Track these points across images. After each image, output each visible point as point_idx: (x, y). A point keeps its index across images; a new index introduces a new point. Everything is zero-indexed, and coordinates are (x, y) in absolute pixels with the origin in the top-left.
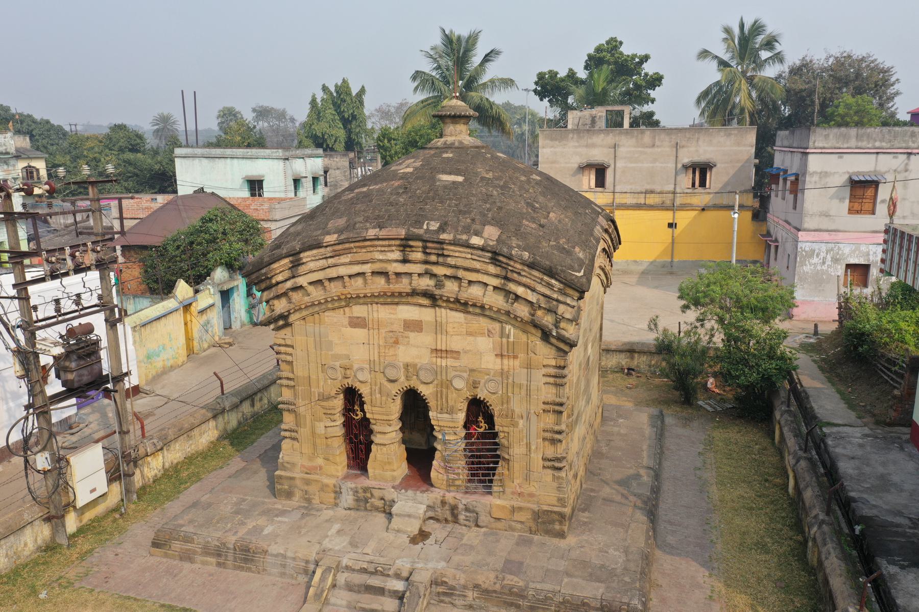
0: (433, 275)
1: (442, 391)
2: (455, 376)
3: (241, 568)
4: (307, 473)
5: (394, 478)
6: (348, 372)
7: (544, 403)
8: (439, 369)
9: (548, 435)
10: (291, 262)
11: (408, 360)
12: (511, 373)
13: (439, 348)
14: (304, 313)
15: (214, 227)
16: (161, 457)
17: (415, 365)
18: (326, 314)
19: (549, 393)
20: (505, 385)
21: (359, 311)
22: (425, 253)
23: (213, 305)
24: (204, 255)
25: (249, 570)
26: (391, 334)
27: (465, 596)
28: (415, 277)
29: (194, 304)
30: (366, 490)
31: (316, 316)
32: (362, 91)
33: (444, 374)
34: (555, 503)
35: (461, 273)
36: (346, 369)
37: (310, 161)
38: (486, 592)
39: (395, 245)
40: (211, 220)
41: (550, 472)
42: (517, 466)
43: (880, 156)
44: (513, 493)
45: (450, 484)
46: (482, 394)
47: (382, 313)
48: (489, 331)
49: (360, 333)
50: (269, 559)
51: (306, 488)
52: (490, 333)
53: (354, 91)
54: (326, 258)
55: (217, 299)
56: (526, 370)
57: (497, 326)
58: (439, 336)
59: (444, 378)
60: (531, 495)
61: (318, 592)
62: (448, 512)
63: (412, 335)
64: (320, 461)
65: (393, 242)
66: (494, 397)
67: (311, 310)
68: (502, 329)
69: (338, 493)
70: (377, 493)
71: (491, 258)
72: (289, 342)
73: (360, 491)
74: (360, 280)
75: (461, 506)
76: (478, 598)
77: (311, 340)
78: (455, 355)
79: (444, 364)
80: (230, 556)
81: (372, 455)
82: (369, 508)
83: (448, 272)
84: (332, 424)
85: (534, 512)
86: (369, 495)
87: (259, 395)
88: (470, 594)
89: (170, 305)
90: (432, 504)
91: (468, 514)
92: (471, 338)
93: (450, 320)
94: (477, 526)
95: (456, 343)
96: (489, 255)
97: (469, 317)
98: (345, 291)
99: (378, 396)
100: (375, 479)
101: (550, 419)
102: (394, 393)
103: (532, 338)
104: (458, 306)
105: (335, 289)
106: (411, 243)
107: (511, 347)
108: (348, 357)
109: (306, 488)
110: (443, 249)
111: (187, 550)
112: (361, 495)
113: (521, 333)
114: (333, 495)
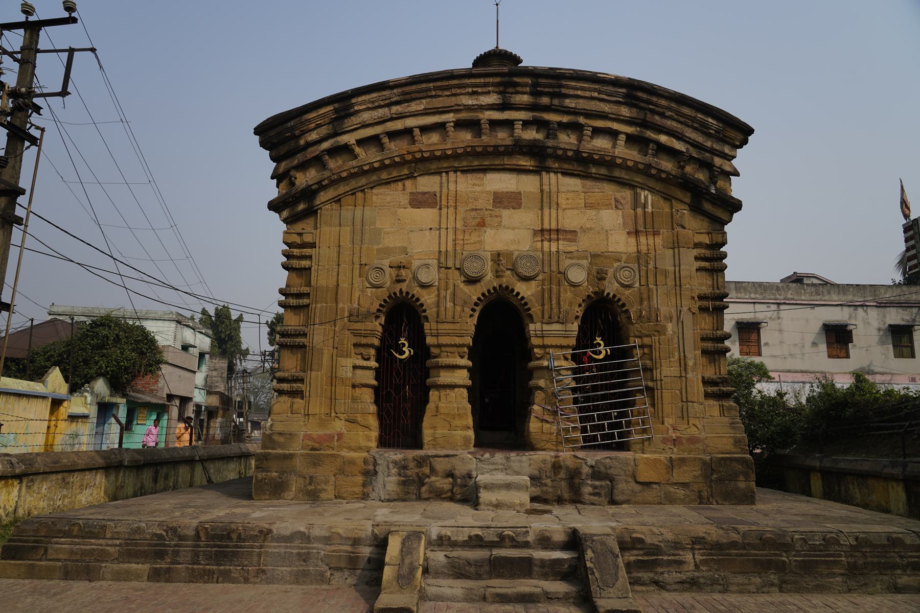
0: (540, 124)
1: (550, 290)
2: (572, 265)
3: (206, 577)
4: (312, 450)
5: (466, 439)
6: (403, 272)
7: (701, 298)
8: (546, 258)
9: (709, 345)
10: (336, 111)
11: (499, 247)
12: (652, 256)
13: (546, 226)
14: (342, 189)
15: (105, 332)
16: (15, 492)
17: (509, 254)
18: (375, 191)
19: (702, 284)
20: (643, 273)
21: (427, 184)
22: (535, 93)
23: (85, 417)
24: (86, 362)
25: (226, 577)
26: (474, 213)
27: (680, 563)
28: (518, 126)
29: (65, 404)
30: (420, 462)
31: (360, 195)
32: (240, 319)
33: (554, 263)
34: (730, 447)
35: (582, 120)
36: (400, 267)
37: (199, 336)
38: (718, 547)
39: (493, 85)
40: (103, 325)
41: (712, 402)
42: (668, 398)
43: (757, 305)
44: (665, 441)
45: (563, 440)
46: (611, 288)
47: (463, 184)
48: (616, 201)
49: (427, 215)
50: (273, 548)
51: (312, 471)
52: (618, 205)
53: (234, 316)
54: (389, 105)
55: (93, 411)
56: (671, 251)
57: (627, 194)
58: (546, 211)
59: (554, 268)
60: (693, 440)
61: (405, 571)
62: (563, 484)
63: (505, 213)
64: (339, 426)
65: (491, 80)
66: (627, 292)
67: (353, 184)
68: (636, 197)
69: (370, 474)
70: (441, 465)
71: (626, 96)
72: (308, 238)
73: (412, 465)
74: (435, 138)
75: (586, 470)
76: (704, 562)
77: (347, 229)
78: (569, 236)
79: (554, 249)
80: (185, 554)
81: (431, 406)
82: (424, 496)
83: (565, 119)
84: (365, 363)
85: (704, 463)
86: (427, 470)
87: (164, 471)
88: (688, 557)
89: (38, 388)
90: (536, 473)
91: (597, 483)
92: (592, 213)
93: (562, 189)
94: (613, 502)
95: (570, 220)
96: (624, 90)
97: (589, 183)
98: (414, 148)
99: (449, 305)
100: (435, 446)
101: (706, 323)
102: (475, 298)
103: (677, 206)
104: (574, 167)
105: (396, 148)
106: (517, 80)
107: (649, 220)
108: (404, 250)
109: (312, 471)
110: (562, 86)
111: (84, 553)
112: (412, 472)
113: (662, 201)
114: (360, 479)
